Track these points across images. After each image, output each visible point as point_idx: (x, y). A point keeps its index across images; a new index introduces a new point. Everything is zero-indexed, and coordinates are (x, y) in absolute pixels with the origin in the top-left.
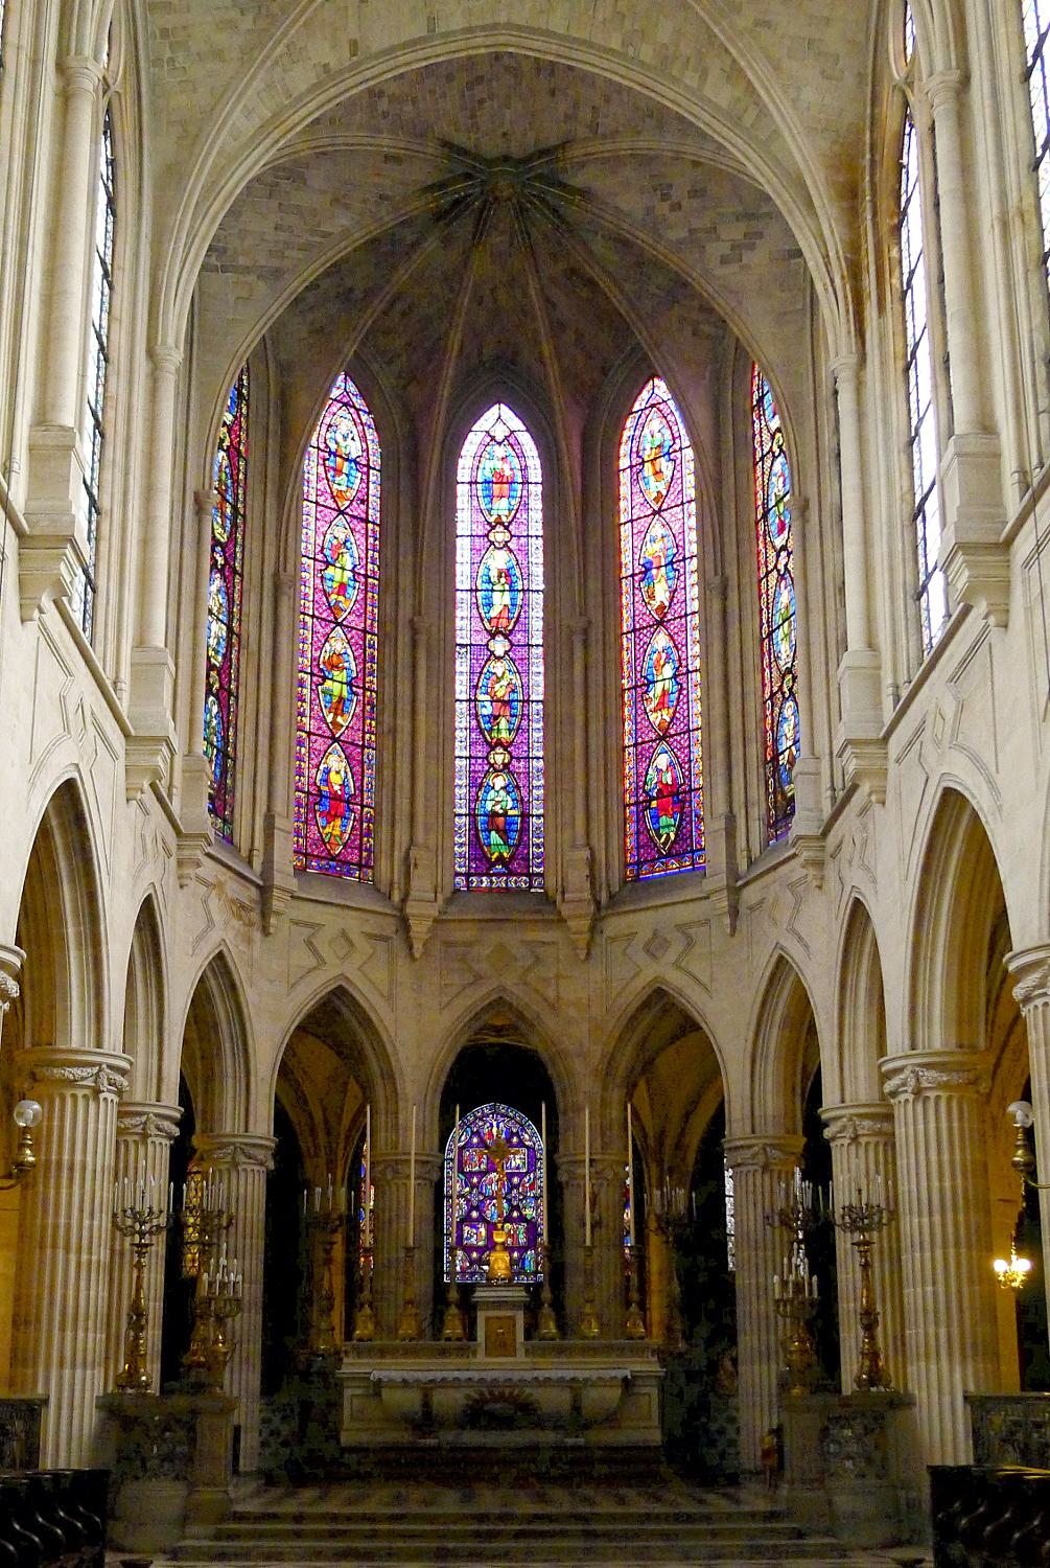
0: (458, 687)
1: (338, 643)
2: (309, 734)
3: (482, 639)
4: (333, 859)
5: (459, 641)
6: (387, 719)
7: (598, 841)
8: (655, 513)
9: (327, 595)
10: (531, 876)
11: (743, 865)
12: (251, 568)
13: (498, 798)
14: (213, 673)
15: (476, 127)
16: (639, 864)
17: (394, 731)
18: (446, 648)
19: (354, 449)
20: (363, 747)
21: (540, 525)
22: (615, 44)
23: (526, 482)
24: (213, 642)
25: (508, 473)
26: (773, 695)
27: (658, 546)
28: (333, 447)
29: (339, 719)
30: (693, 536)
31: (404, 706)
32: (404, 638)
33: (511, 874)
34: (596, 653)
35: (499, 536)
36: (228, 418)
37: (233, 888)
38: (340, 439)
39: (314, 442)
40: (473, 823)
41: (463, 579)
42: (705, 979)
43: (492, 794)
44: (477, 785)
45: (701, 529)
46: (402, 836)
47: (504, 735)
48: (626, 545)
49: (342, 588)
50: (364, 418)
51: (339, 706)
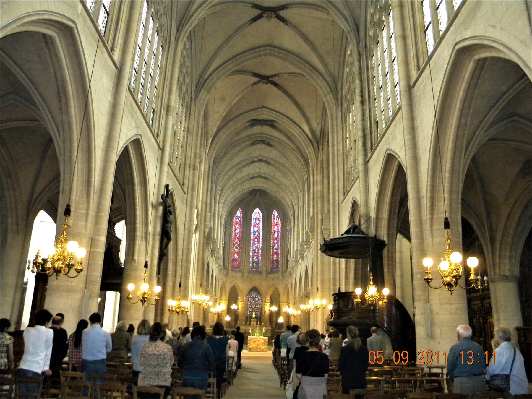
1: (236, 241)
13: (255, 259)
16: (272, 269)
22: (270, 188)
37: (225, 273)
41: (252, 231)
44: (253, 258)
46: (244, 264)
48: (272, 228)
49: (237, 233)
51: (237, 248)
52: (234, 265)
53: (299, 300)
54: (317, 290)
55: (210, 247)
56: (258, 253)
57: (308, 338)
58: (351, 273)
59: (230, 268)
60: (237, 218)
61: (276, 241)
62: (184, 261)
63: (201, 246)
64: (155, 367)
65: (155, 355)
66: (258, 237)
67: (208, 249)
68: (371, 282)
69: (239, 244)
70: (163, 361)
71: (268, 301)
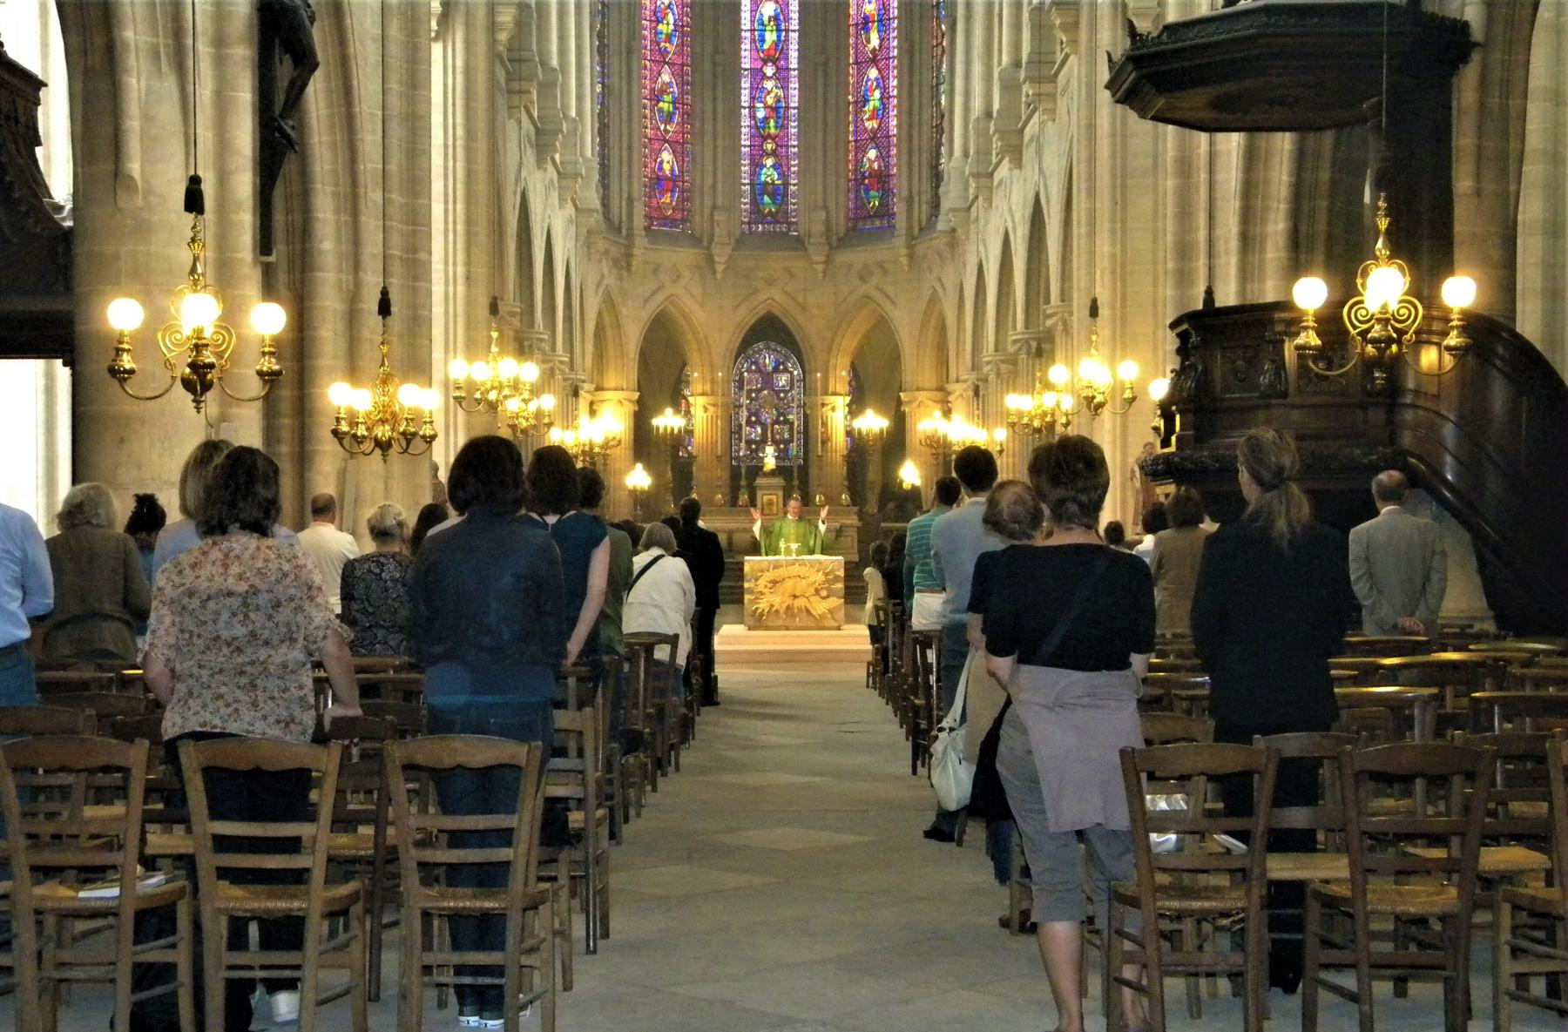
0: (743, 98)
1: (666, 77)
2: (650, 139)
3: (759, 65)
4: (666, 218)
5: (743, 66)
6: (698, 124)
7: (832, 207)
9: (658, 44)
10: (789, 224)
11: (916, 230)
12: (613, 40)
17: (702, 133)
18: (735, 72)
20: (683, 144)
31: (709, 115)
32: (707, 66)
41: (746, 23)
42: (892, 295)
43: (764, 170)
44: (757, 165)
47: (773, 131)
49: (669, 39)
51: (669, 118)
52: (659, 208)
53: (998, 375)
54: (1094, 311)
55: (531, 117)
56: (781, 141)
57: (1046, 487)
58: (1272, 217)
59: (639, 222)
62: (394, 180)
63: (481, 105)
64: (239, 650)
65: (230, 594)
66: (776, 55)
67: (519, 122)
68: (1380, 244)
69: (682, 93)
70: (270, 617)
71: (843, 387)
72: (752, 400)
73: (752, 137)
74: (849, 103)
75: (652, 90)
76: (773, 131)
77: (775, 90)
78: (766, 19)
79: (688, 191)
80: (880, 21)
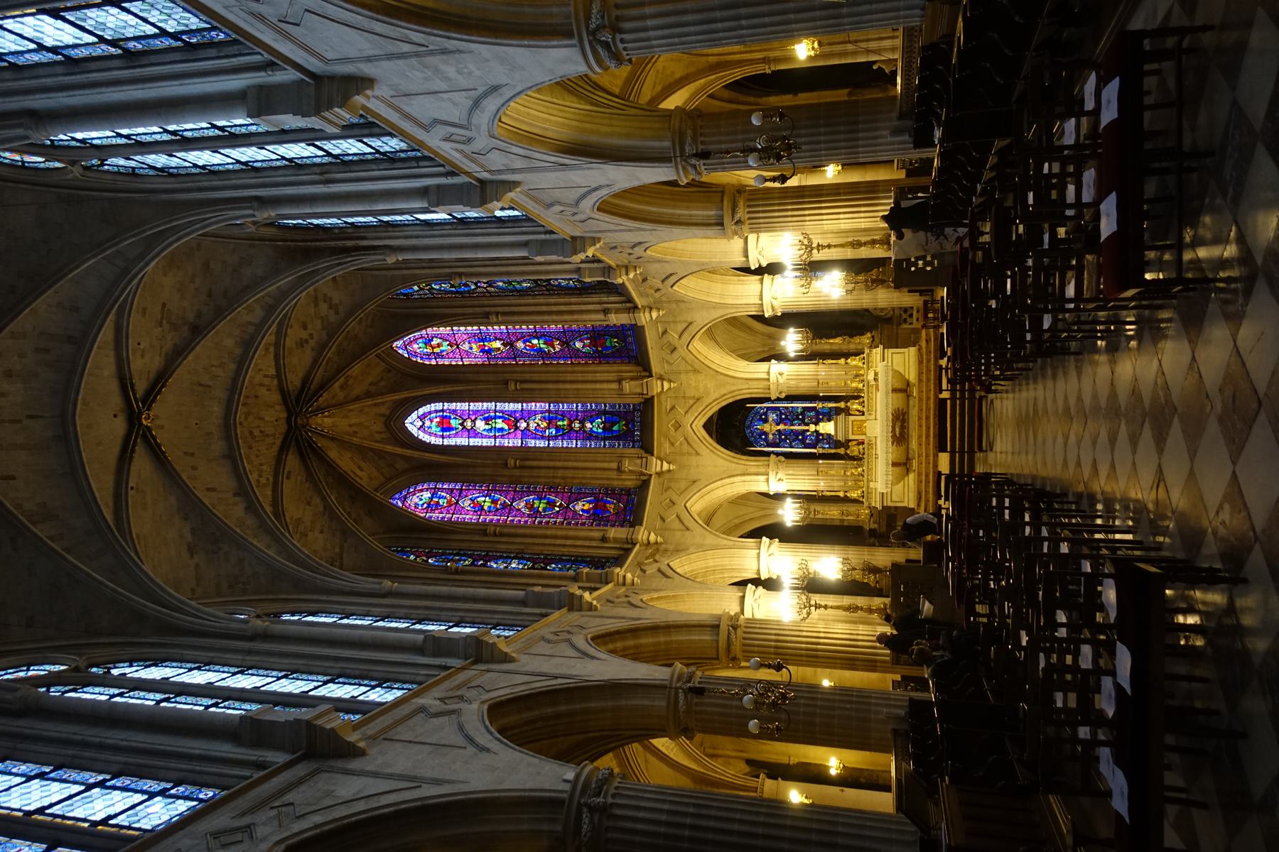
0: (542, 445)
5: (519, 445)
6: (557, 481)
8: (458, 347)
9: (497, 510)
13: (596, 426)
14: (536, 566)
15: (274, 435)
17: (564, 478)
18: (524, 450)
19: (427, 495)
20: (571, 493)
21: (463, 404)
23: (443, 411)
24: (521, 567)
25: (438, 419)
26: (548, 290)
27: (474, 346)
28: (425, 505)
29: (558, 504)
30: (469, 328)
31: (551, 472)
33: (633, 421)
34: (527, 376)
35: (469, 424)
36: (412, 557)
38: (421, 503)
39: (422, 515)
40: (609, 439)
43: (595, 429)
44: (590, 436)
45: (465, 325)
46: (613, 475)
47: (565, 423)
49: (494, 502)
50: (412, 490)
51: (551, 504)
56: (572, 417)
60: (431, 506)
61: (520, 345)
69: (534, 492)
71: (763, 366)
72: (786, 438)
73: (570, 438)
74: (544, 363)
75: (529, 516)
76: (565, 423)
77: (536, 421)
78: (487, 427)
79: (607, 489)
80: (483, 340)
